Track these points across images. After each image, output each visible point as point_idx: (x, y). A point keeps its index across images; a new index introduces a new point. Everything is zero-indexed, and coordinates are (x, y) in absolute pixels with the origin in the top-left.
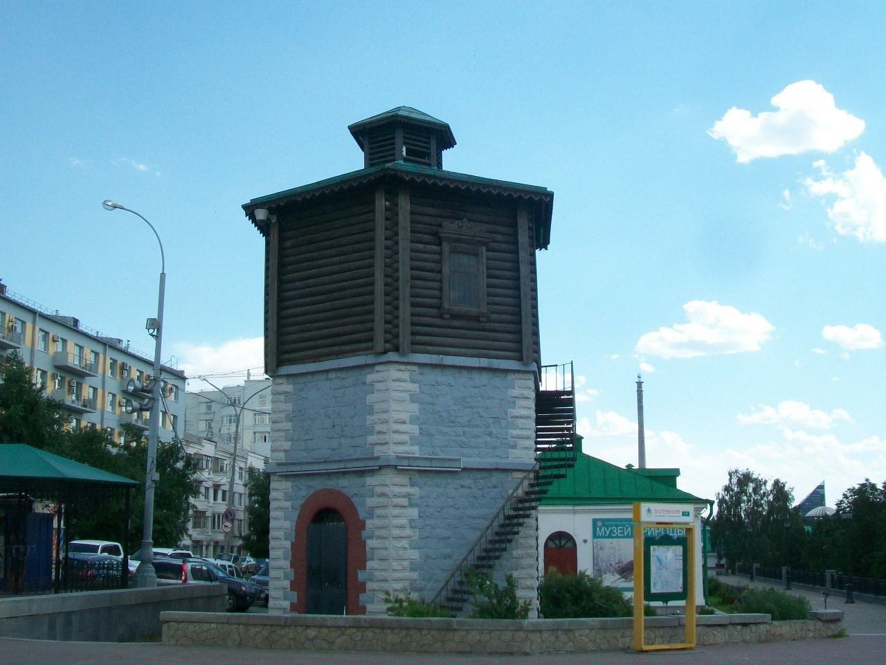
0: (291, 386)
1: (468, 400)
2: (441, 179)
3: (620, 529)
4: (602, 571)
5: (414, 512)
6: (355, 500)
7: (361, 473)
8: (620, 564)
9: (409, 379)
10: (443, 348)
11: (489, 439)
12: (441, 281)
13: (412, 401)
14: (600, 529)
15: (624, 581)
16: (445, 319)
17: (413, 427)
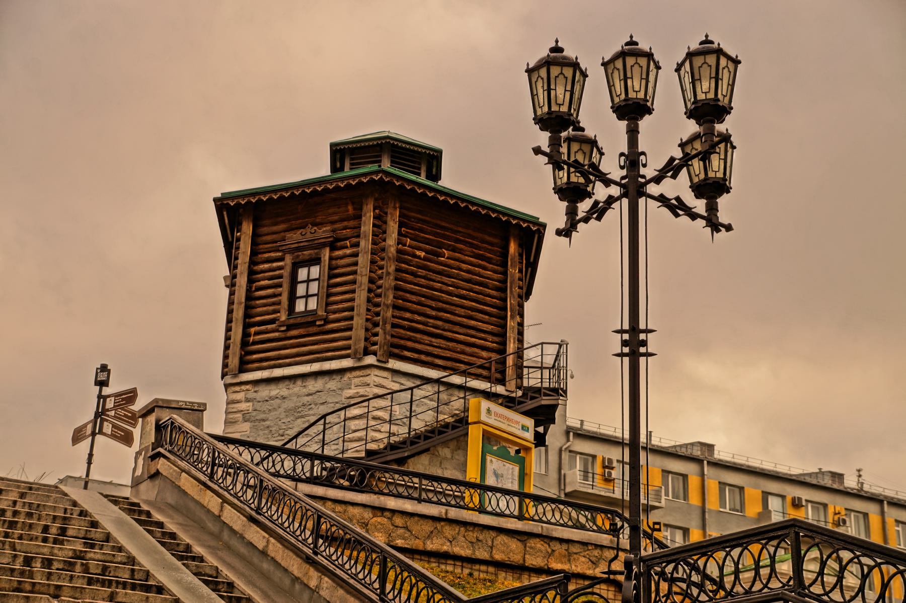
1: (300, 409)
2: (442, 193)
13: (245, 420)
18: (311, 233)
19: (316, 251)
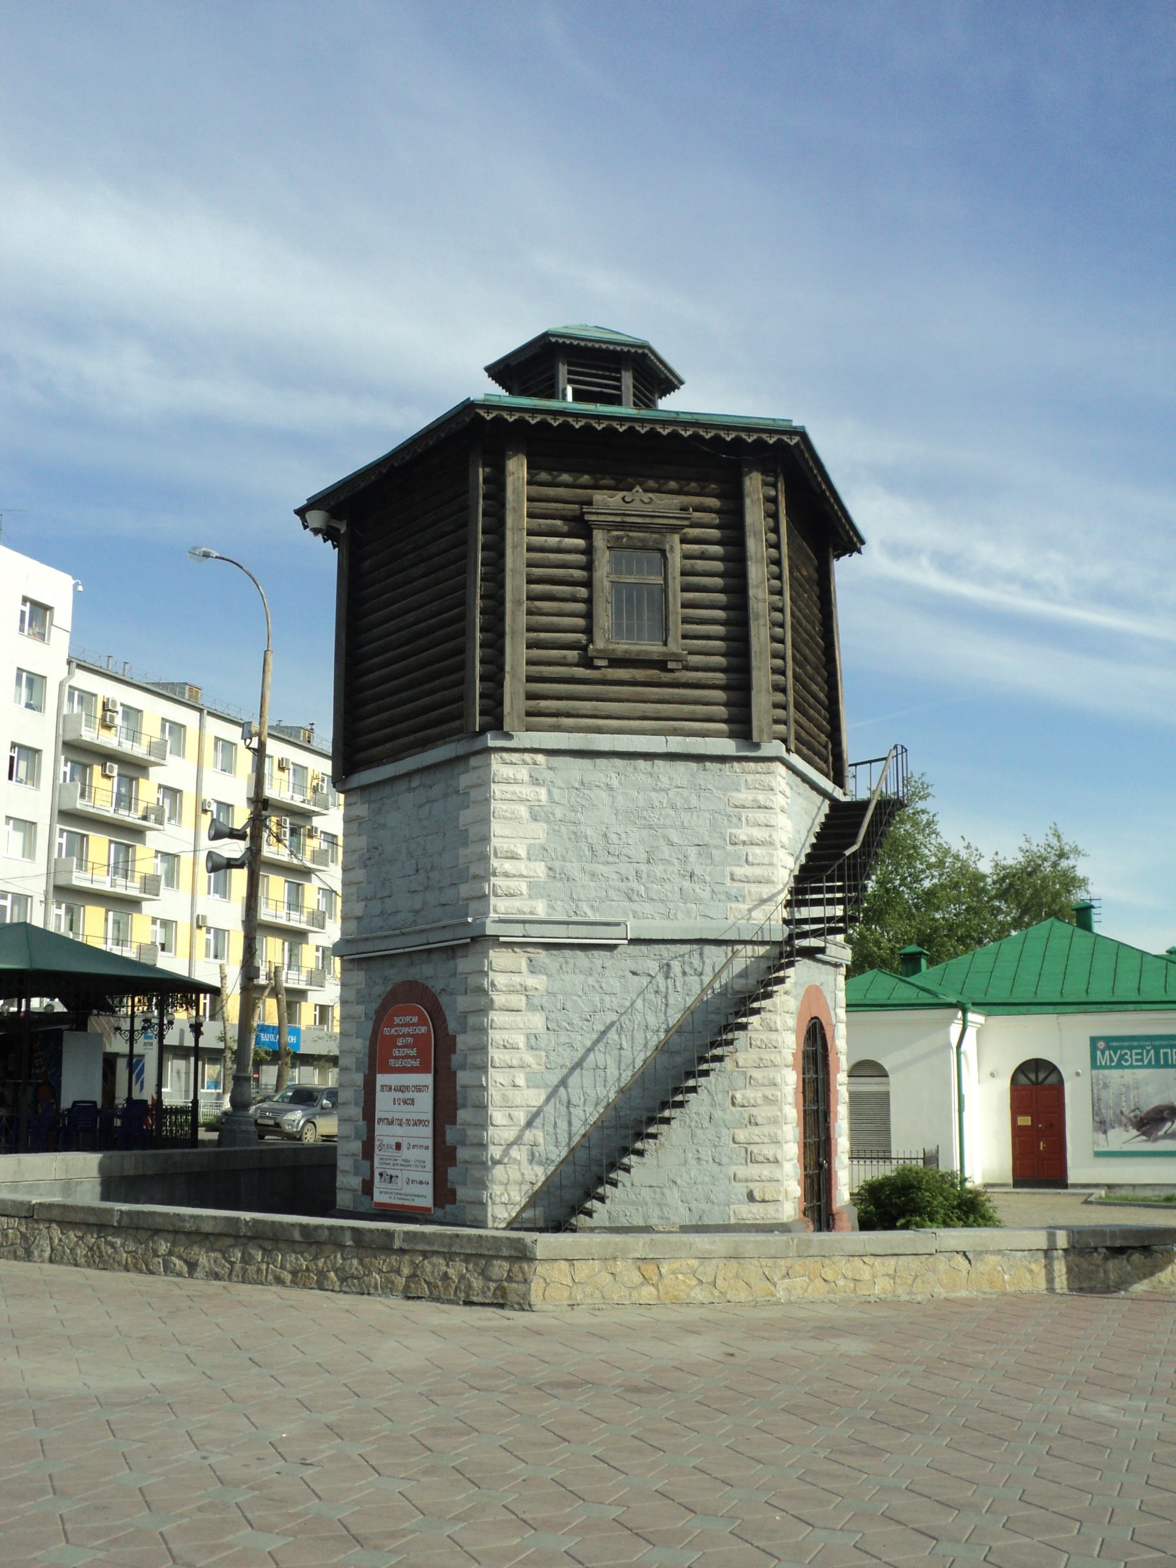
0: (367, 805)
3: (1137, 1054)
4: (1108, 1125)
5: (537, 1021)
6: (443, 1000)
7: (452, 951)
8: (1138, 1113)
9: (526, 778)
10: (596, 722)
11: (686, 884)
12: (589, 601)
13: (535, 818)
14: (1103, 1053)
15: (1145, 1141)
16: (598, 668)
17: (532, 865)
18: (642, 501)
19: (655, 536)
